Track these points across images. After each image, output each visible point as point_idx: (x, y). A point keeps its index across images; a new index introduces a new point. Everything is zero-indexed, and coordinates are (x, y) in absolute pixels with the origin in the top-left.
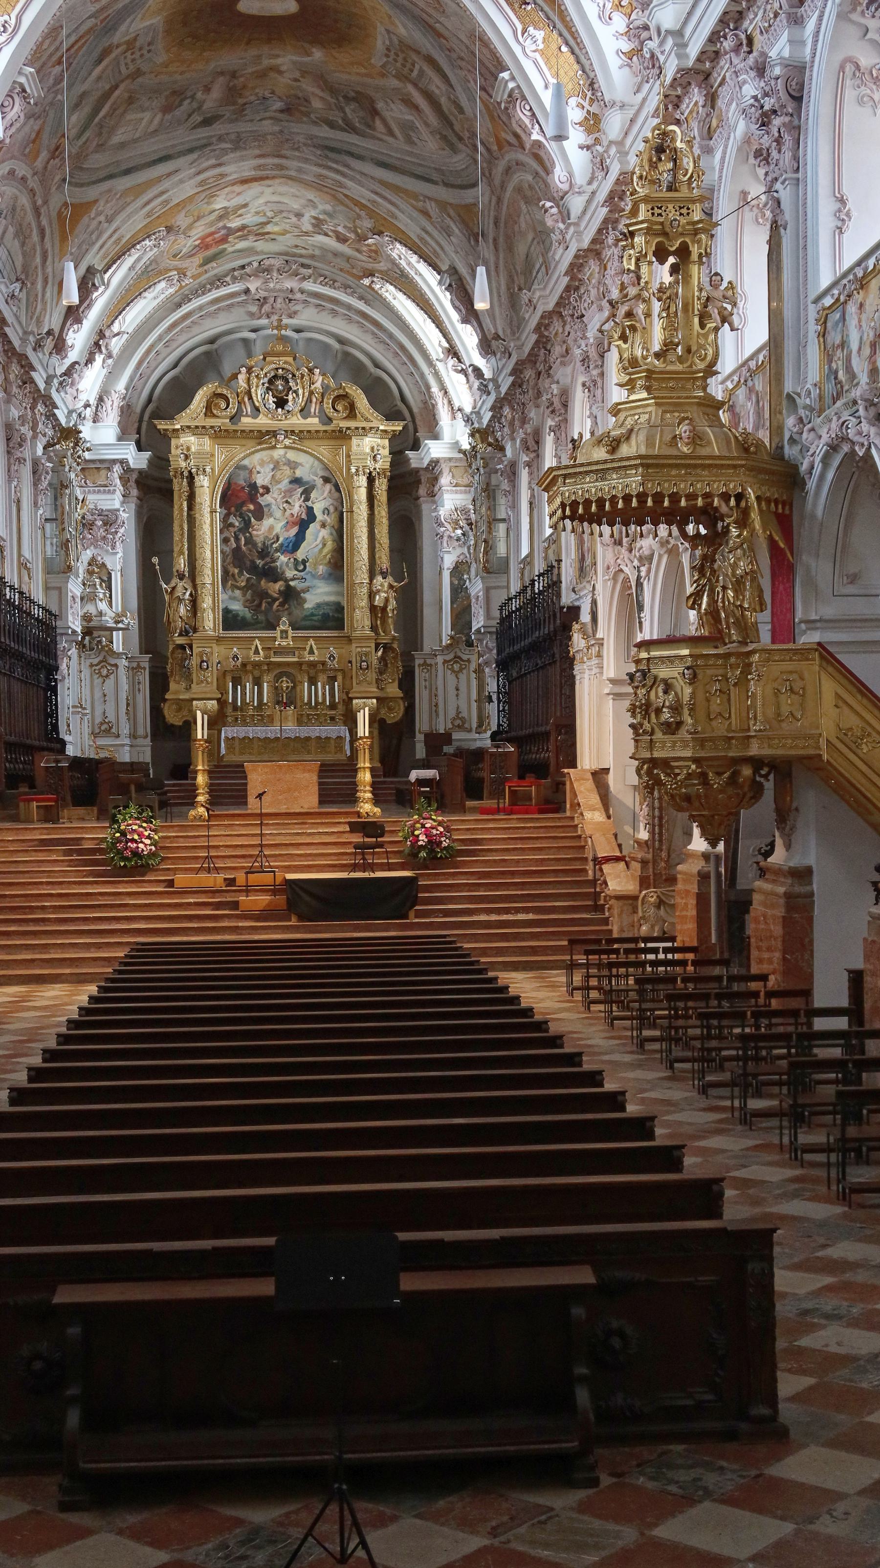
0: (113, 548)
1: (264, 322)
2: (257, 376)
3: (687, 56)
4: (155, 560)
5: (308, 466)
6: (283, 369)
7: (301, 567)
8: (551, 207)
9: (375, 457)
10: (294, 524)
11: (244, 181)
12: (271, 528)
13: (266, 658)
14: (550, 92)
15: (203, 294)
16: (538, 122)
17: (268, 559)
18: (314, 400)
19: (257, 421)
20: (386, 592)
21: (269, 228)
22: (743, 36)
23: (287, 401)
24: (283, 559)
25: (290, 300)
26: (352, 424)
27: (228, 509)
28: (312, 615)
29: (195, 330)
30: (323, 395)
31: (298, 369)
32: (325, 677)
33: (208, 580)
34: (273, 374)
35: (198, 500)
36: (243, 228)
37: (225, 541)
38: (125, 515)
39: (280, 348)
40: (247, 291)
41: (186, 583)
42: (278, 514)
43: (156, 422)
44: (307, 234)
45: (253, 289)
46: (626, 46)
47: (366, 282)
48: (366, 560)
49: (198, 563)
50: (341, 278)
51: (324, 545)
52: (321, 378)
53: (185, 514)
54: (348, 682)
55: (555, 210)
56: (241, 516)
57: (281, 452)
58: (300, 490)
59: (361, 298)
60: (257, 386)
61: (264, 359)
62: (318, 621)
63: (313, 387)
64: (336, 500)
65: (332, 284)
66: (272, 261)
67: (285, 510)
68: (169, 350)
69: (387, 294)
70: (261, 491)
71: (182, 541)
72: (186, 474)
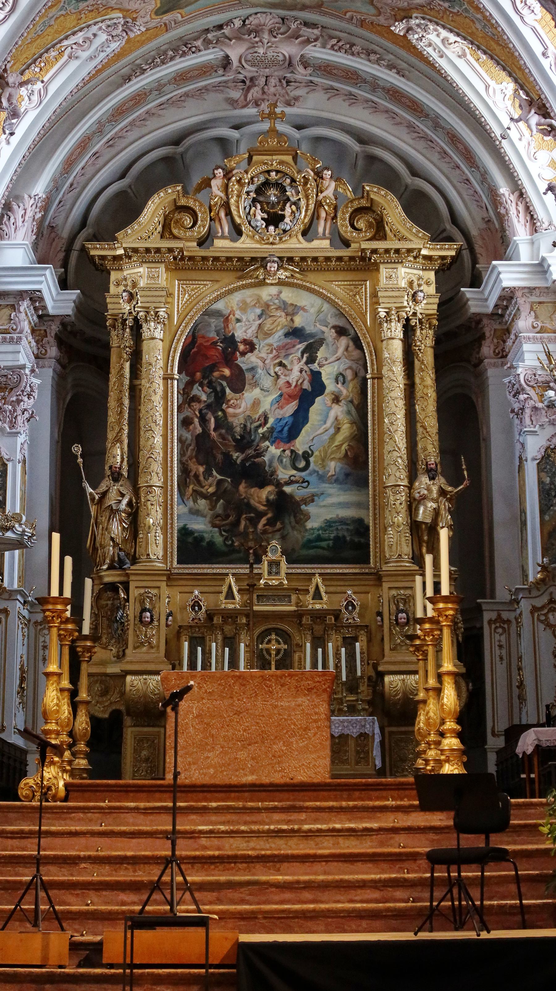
0: (12, 426)
2: (239, 181)
4: (77, 449)
5: (313, 310)
6: (278, 172)
7: (302, 464)
9: (414, 295)
10: (291, 397)
12: (256, 403)
13: (244, 605)
15: (163, 63)
17: (251, 452)
18: (323, 214)
19: (238, 245)
20: (435, 501)
23: (283, 217)
24: (274, 451)
25: (288, 82)
26: (380, 245)
27: (191, 374)
28: (319, 539)
29: (151, 123)
30: (336, 208)
31: (299, 172)
32: (340, 639)
33: (157, 481)
34: (262, 179)
35: (145, 357)
37: (185, 423)
38: (36, 381)
39: (273, 143)
40: (226, 62)
41: (123, 486)
42: (267, 382)
43: (89, 245)
47: (399, 28)
48: (404, 451)
49: (143, 454)
51: (338, 430)
52: (333, 184)
53: (127, 382)
54: (376, 649)
56: (210, 384)
57: (274, 290)
58: (301, 346)
59: (391, 67)
60: (239, 196)
61: (250, 158)
62: (329, 548)
63: (321, 196)
64: (356, 361)
66: (261, 19)
67: (278, 376)
68: (114, 151)
69: (430, 50)
70: (242, 347)
71: (119, 422)
72: (130, 322)
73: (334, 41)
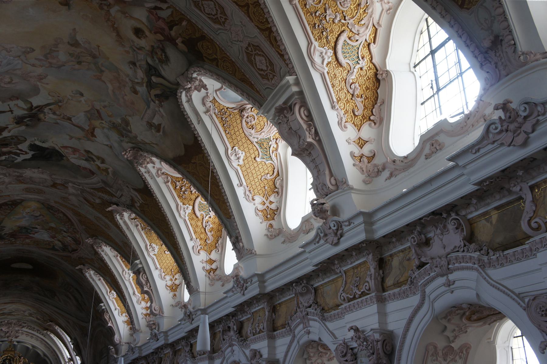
1: (6, 339)
3: (168, 340)
6: (9, 356)
8: (112, 348)
11: (5, 303)
14: (117, 311)
16: (111, 320)
21: (13, 313)
22: (189, 344)
36: (3, 313)
44: (26, 316)
45: (3, 329)
46: (145, 312)
50: (36, 328)
55: (113, 350)
59: (42, 335)
65: (33, 329)
73: (30, 327)
